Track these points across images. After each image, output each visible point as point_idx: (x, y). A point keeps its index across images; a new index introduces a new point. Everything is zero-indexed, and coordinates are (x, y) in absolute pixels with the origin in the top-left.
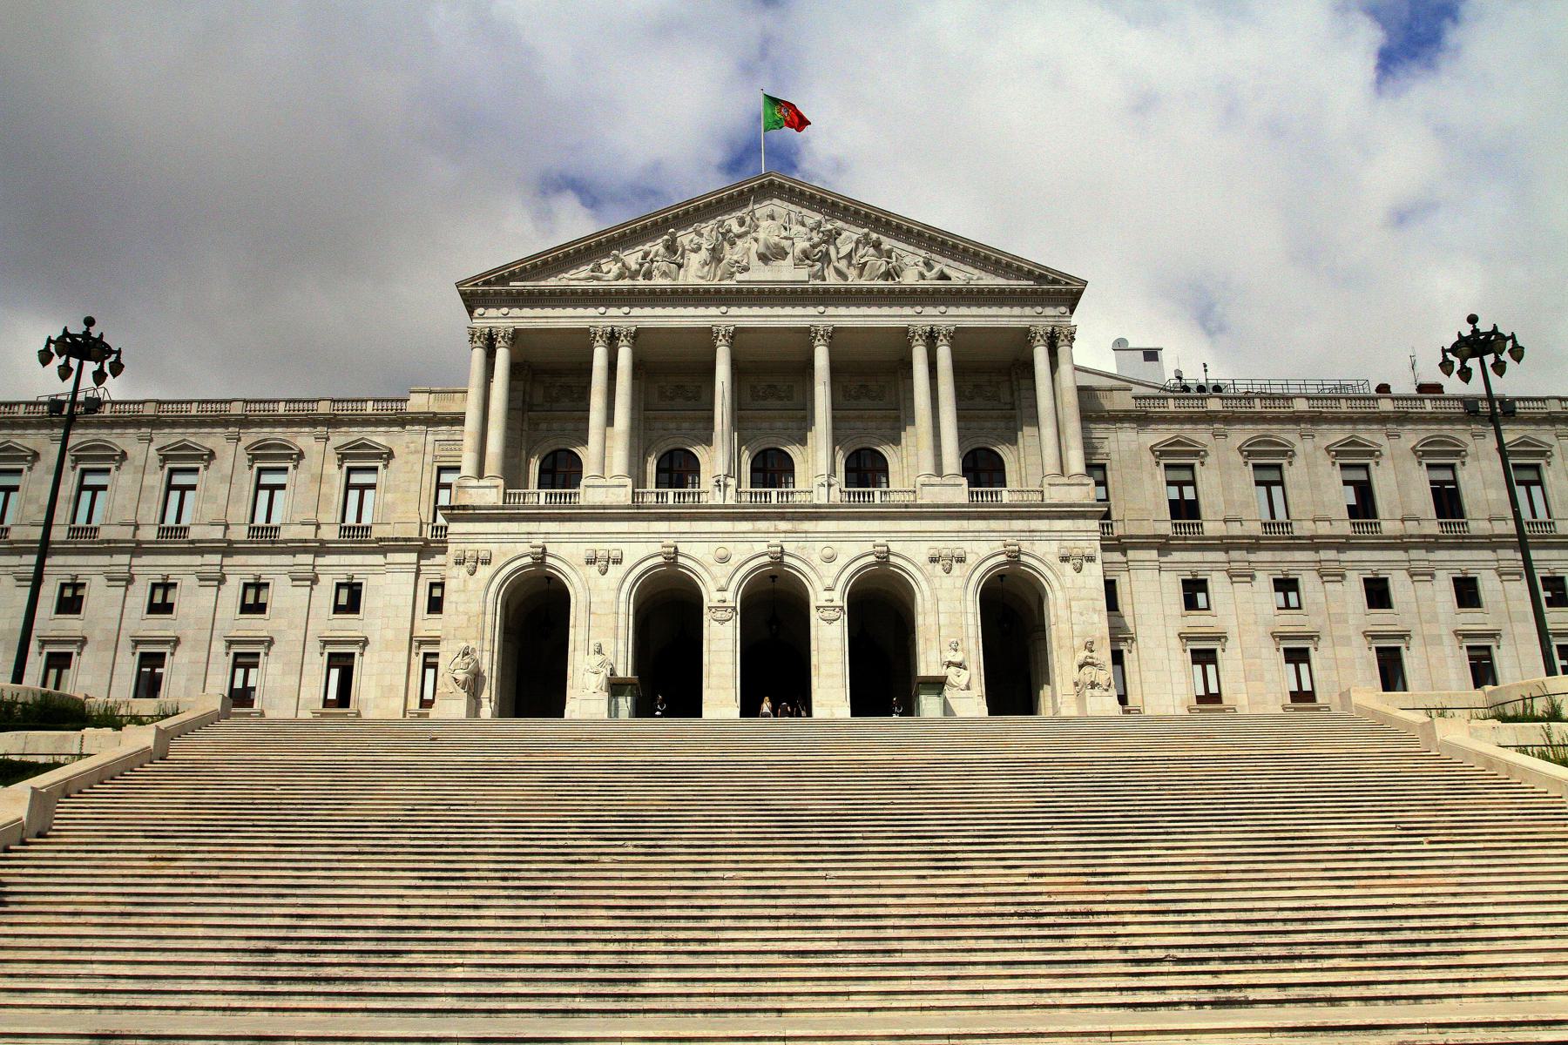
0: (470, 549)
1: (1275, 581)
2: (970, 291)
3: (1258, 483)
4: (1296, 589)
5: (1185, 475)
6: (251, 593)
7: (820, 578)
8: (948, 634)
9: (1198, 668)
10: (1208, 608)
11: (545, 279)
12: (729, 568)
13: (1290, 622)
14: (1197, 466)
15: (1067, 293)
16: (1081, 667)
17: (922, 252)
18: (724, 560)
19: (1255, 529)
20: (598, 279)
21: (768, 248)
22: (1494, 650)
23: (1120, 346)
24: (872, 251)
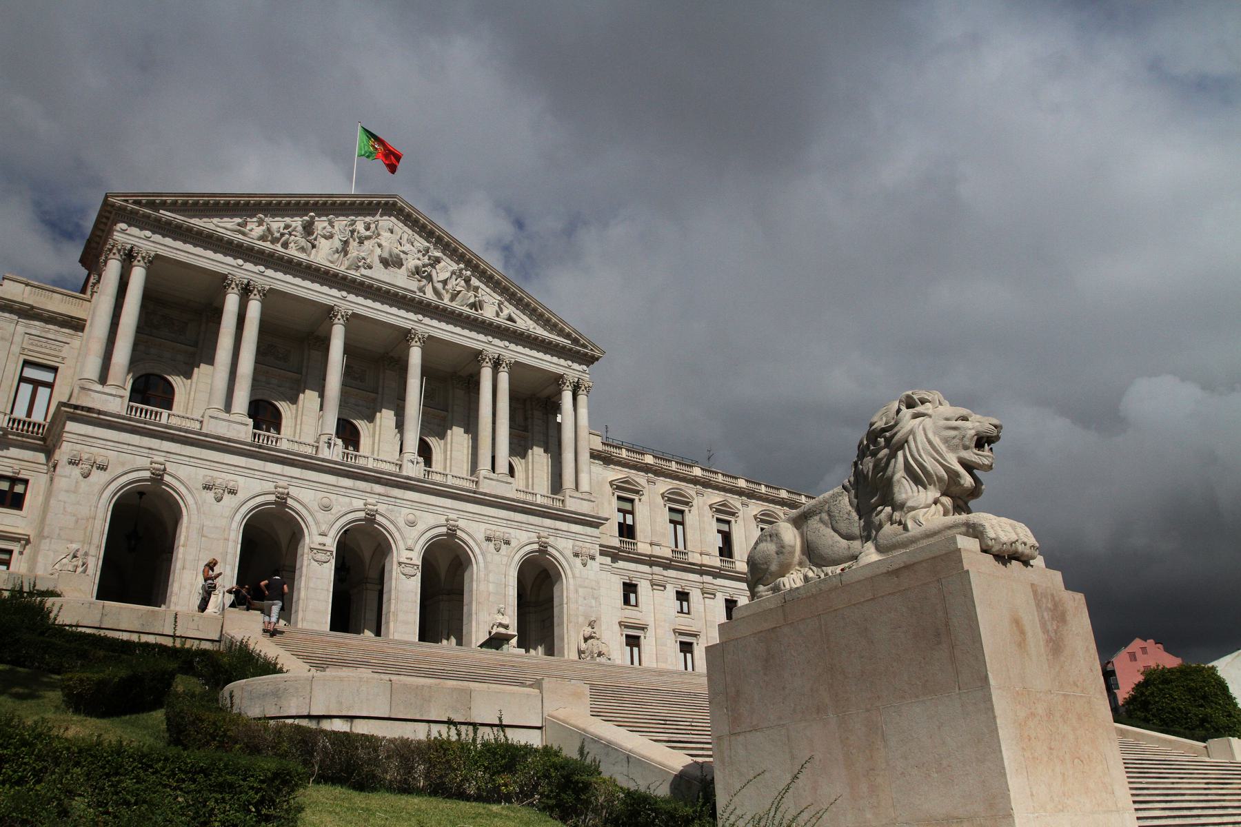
0: (86, 452)
1: (678, 592)
4: (687, 600)
5: (627, 506)
7: (403, 538)
8: (492, 599)
10: (636, 606)
11: (191, 217)
12: (330, 517)
13: (684, 622)
14: (637, 501)
16: (586, 640)
19: (668, 554)
20: (244, 234)
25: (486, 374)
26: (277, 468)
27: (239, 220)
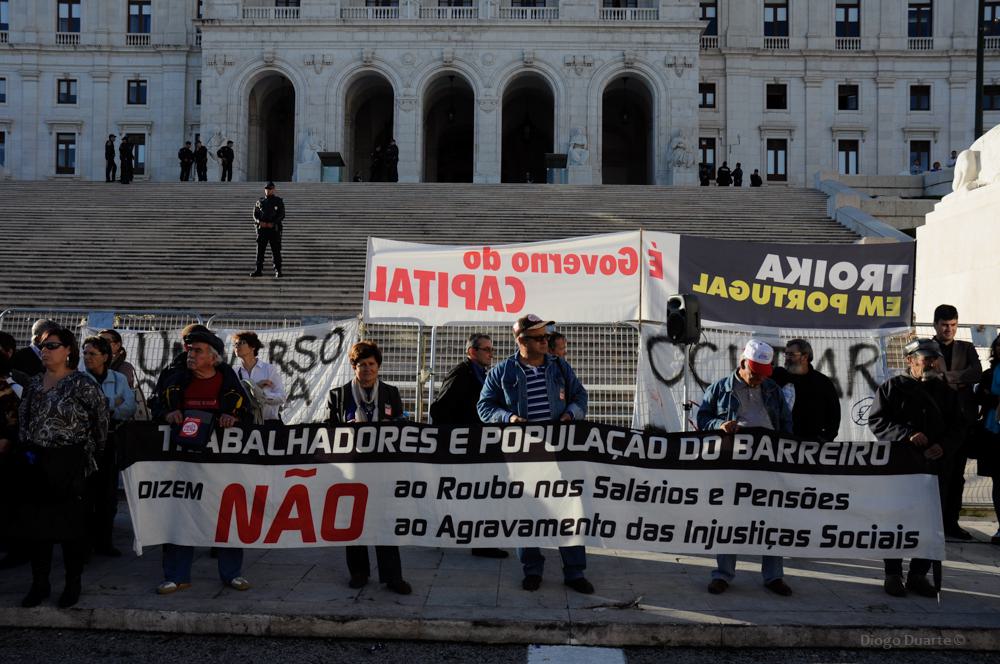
6: (64, 86)
8: (579, 122)
26: (362, 36)
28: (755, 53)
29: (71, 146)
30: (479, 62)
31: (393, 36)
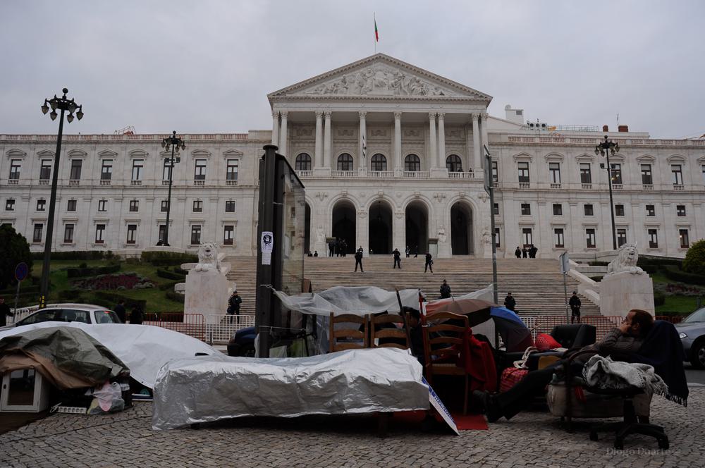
2: (451, 100)
3: (550, 169)
6: (196, 204)
9: (525, 235)
15: (486, 101)
16: (484, 235)
17: (434, 84)
18: (363, 196)
19: (548, 186)
20: (318, 94)
21: (379, 83)
22: (627, 231)
23: (508, 108)
24: (416, 84)
25: (432, 123)
26: (342, 184)
27: (315, 87)
28: (515, 191)
29: (198, 232)
30: (395, 196)
31: (356, 184)
